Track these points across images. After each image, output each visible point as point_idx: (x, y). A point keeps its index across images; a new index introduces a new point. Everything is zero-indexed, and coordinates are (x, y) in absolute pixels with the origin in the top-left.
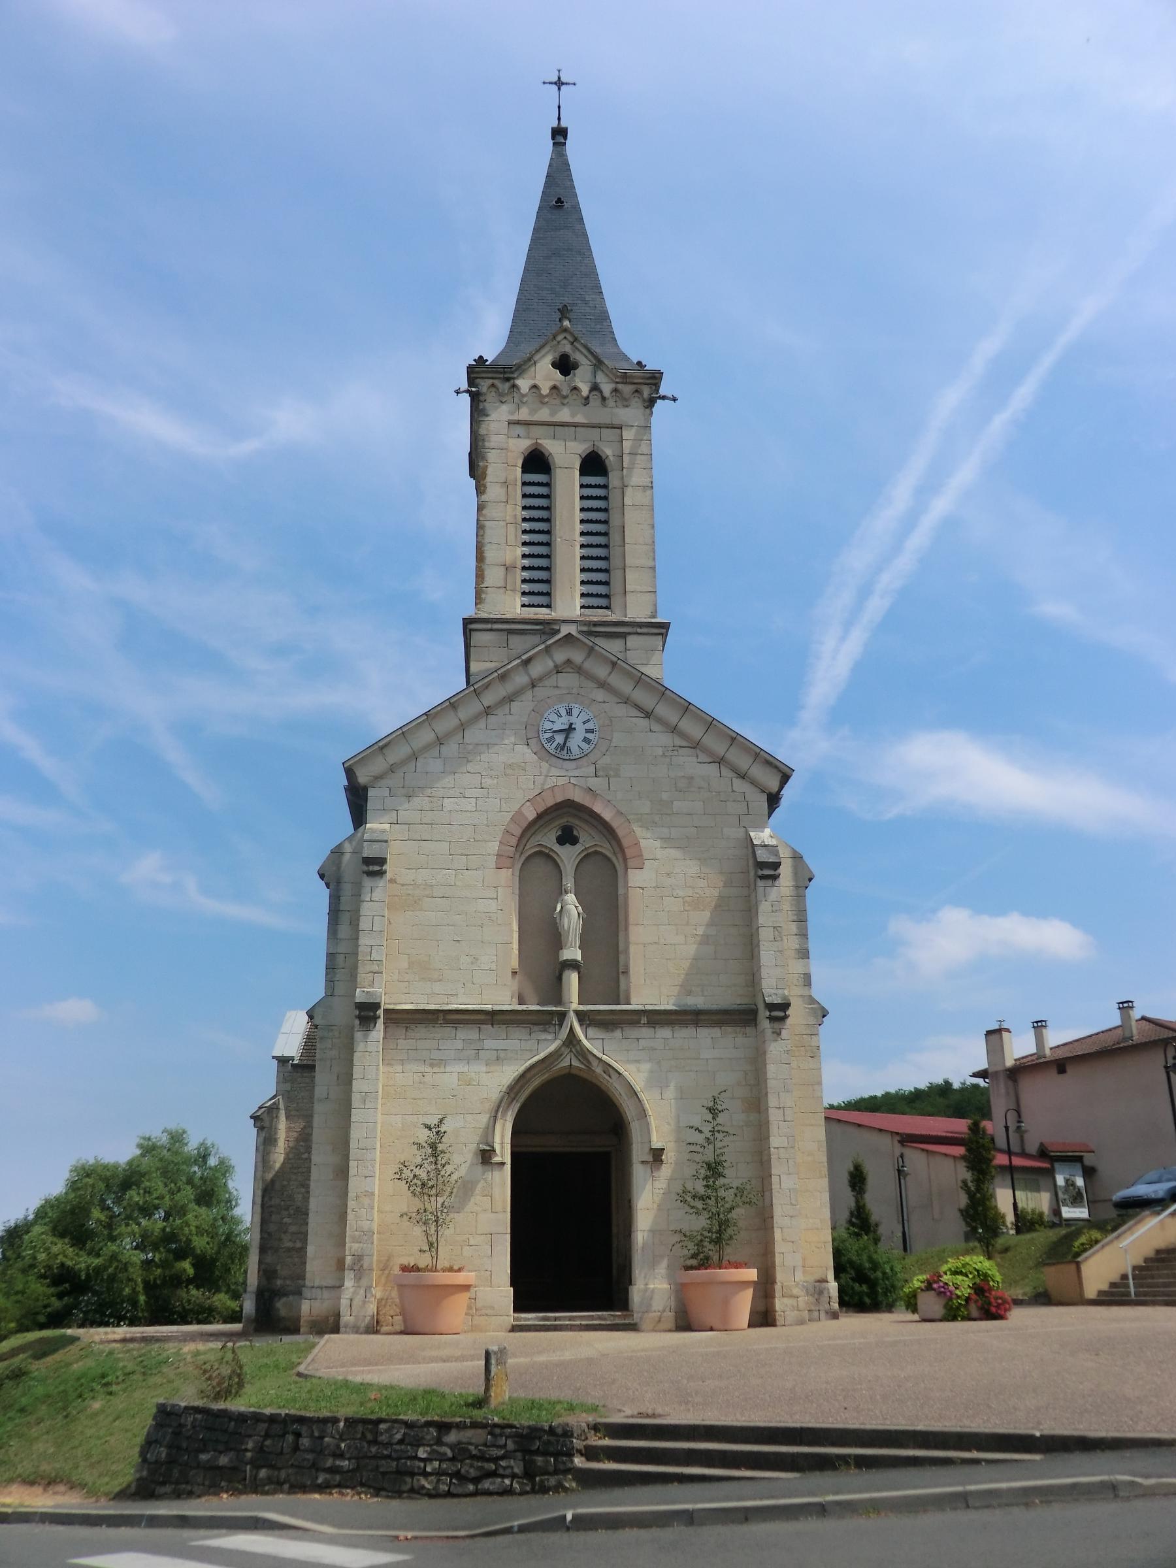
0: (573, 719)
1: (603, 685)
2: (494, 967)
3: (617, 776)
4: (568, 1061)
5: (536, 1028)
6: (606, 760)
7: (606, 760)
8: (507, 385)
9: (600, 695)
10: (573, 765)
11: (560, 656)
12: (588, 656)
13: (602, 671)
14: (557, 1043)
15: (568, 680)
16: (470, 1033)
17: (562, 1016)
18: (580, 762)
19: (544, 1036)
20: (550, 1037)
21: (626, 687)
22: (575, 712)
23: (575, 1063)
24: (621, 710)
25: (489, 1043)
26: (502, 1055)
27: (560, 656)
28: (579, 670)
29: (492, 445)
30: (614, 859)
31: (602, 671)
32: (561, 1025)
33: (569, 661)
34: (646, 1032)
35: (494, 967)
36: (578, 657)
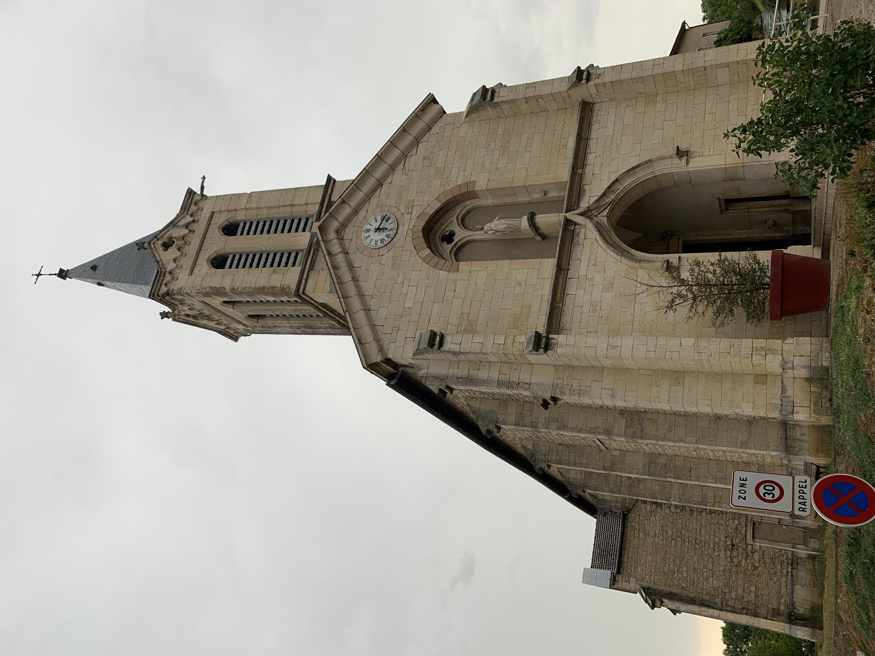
0: (373, 228)
1: (356, 212)
2: (525, 271)
3: (413, 201)
4: (603, 218)
5: (575, 241)
6: (402, 208)
7: (402, 208)
8: (167, 275)
9: (362, 213)
10: (401, 228)
11: (332, 235)
12: (336, 219)
13: (347, 210)
14: (589, 224)
15: (348, 233)
16: (572, 287)
17: (568, 222)
18: (400, 224)
19: (582, 235)
20: (583, 231)
21: (359, 196)
22: (369, 227)
23: (605, 213)
24: (374, 200)
25: (582, 271)
26: (593, 262)
27: (332, 235)
28: (344, 225)
29: (199, 285)
30: (468, 208)
31: (347, 210)
32: (575, 224)
33: (337, 231)
34: (588, 170)
35: (525, 271)
36: (335, 225)
